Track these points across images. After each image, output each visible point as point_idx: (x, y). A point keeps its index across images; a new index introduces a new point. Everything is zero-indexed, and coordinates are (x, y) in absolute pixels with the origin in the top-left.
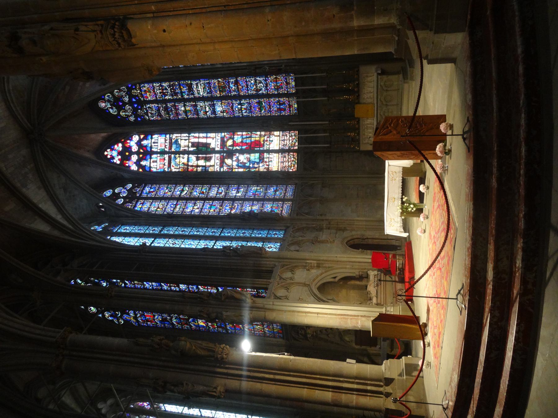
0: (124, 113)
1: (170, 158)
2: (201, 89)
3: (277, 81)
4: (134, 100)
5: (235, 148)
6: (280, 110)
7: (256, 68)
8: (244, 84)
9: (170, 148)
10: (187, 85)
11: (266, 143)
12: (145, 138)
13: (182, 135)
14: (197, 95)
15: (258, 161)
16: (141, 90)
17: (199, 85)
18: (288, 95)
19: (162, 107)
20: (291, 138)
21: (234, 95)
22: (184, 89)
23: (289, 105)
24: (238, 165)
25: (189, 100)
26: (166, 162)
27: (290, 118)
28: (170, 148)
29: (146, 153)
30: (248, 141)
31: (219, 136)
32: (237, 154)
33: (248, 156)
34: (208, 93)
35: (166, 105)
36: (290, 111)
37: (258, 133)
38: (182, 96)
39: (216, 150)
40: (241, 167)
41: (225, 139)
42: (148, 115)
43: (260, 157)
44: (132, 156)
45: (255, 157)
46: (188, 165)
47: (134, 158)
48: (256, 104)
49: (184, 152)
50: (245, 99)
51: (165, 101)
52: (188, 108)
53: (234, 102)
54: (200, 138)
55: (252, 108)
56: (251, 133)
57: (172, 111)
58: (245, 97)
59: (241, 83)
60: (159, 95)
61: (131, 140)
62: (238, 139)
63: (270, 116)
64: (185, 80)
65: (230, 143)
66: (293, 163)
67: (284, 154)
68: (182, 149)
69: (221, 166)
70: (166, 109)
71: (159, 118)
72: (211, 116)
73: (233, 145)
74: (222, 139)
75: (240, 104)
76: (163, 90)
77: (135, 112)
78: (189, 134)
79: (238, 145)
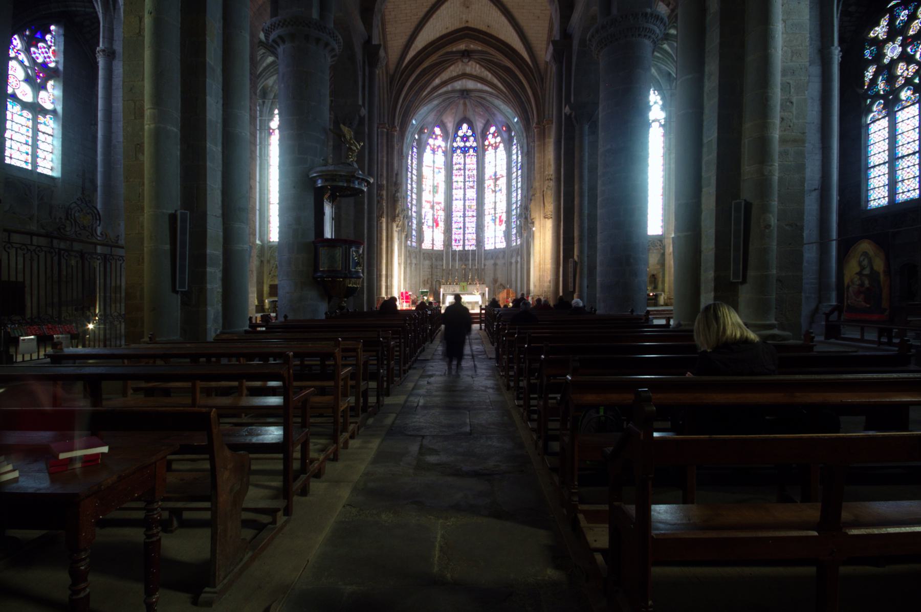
1: (431, 167)
6: (456, 240)
9: (437, 168)
10: (474, 186)
12: (443, 152)
14: (467, 190)
16: (472, 156)
18: (464, 245)
19: (462, 167)
22: (471, 184)
25: (465, 185)
27: (451, 245)
28: (437, 168)
29: (434, 151)
30: (439, 219)
37: (443, 226)
41: (440, 205)
46: (426, 178)
49: (434, 177)
51: (464, 169)
52: (459, 183)
53: (462, 213)
54: (442, 187)
58: (464, 220)
61: (443, 140)
63: (452, 234)
65: (439, 208)
68: (435, 175)
69: (426, 201)
70: (460, 169)
71: (454, 163)
73: (437, 209)
75: (460, 217)
77: (461, 148)
79: (437, 212)
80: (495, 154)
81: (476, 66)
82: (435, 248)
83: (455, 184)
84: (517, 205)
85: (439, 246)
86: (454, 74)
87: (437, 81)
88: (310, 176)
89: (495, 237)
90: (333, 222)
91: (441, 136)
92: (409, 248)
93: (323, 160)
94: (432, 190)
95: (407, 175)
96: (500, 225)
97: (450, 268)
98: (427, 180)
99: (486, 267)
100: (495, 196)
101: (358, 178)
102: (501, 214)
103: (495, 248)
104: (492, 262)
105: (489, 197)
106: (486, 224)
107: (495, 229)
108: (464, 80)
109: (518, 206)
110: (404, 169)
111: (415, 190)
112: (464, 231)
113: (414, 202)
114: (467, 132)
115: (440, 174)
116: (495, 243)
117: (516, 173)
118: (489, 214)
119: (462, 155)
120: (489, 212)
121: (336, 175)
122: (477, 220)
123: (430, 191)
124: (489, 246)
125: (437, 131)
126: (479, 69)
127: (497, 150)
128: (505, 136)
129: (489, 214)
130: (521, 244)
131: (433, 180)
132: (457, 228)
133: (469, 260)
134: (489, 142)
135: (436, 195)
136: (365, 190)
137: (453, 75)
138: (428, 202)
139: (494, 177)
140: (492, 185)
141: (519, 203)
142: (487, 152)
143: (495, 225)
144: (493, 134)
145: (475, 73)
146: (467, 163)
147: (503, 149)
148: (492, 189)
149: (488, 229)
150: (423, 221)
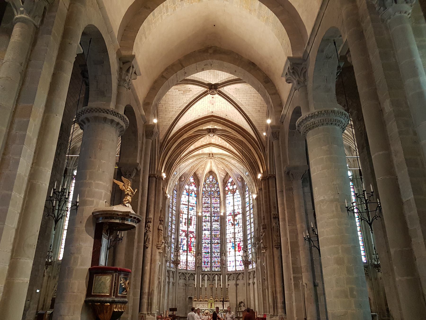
0: (207, 186)
2: (216, 226)
3: (218, 262)
4: (212, 193)
5: (189, 238)
7: (224, 254)
8: (217, 247)
9: (190, 206)
11: (191, 254)
12: (195, 194)
13: (196, 212)
14: (213, 223)
15: (183, 249)
16: (216, 197)
17: (218, 225)
18: (211, 267)
20: (192, 266)
21: (212, 241)
22: (216, 218)
23: (207, 267)
24: (182, 239)
25: (211, 219)
26: (185, 203)
28: (190, 206)
30: (192, 245)
31: (194, 230)
32: (186, 239)
33: (186, 244)
34: (214, 229)
35: (209, 208)
36: (204, 267)
37: (195, 250)
38: (213, 216)
39: (189, 228)
40: (181, 240)
41: (193, 234)
42: (205, 197)
43: (185, 250)
44: (188, 186)
45: (185, 248)
46: (183, 213)
47: (187, 187)
48: (208, 251)
50: (211, 246)
52: (207, 217)
53: (209, 240)
54: (194, 222)
55: (206, 249)
56: (195, 247)
57: (207, 210)
59: (218, 245)
60: (214, 205)
62: (193, 240)
63: (202, 257)
64: (220, 219)
65: (192, 236)
66: (182, 267)
67: (186, 262)
68: (190, 211)
69: (182, 231)
70: (208, 207)
72: (203, 228)
73: (190, 237)
74: (193, 232)
75: (208, 243)
76: (216, 208)
78: (196, 216)
80: (233, 197)
81: (218, 139)
82: (188, 269)
83: (204, 218)
84: (251, 236)
85: (191, 266)
86: (204, 143)
87: (192, 147)
88: (94, 215)
89: (236, 261)
90: (108, 251)
91: (194, 184)
92: (168, 268)
93: (106, 202)
94: (187, 223)
95: (169, 210)
96: (239, 251)
97: (201, 287)
98: (184, 214)
99: (229, 286)
100: (234, 228)
101: (131, 217)
102: (239, 243)
103: (236, 270)
104: (234, 282)
105: (230, 229)
106: (228, 250)
107: (235, 254)
108: (210, 147)
109: (252, 236)
110: (167, 206)
111: (174, 222)
112: (211, 255)
113: (173, 231)
114: (213, 181)
115: (193, 211)
116: (236, 266)
117: (249, 212)
118: (230, 242)
119: (209, 197)
120: (230, 240)
121: (114, 214)
122: (221, 246)
123: (185, 223)
124: (231, 268)
125: (192, 180)
126: (220, 140)
127: (234, 195)
128: (240, 184)
129: (230, 242)
130: (257, 268)
131: (188, 214)
132: (205, 253)
133: (215, 280)
134: (229, 189)
135: (190, 226)
136: (136, 226)
137: (203, 144)
138: (183, 231)
139: (232, 214)
140: (232, 219)
141: (253, 234)
142: (227, 196)
143: (235, 251)
144: (231, 183)
145: (218, 144)
146: (213, 203)
147: (239, 193)
148: (231, 223)
149: (229, 254)
150: (180, 246)
